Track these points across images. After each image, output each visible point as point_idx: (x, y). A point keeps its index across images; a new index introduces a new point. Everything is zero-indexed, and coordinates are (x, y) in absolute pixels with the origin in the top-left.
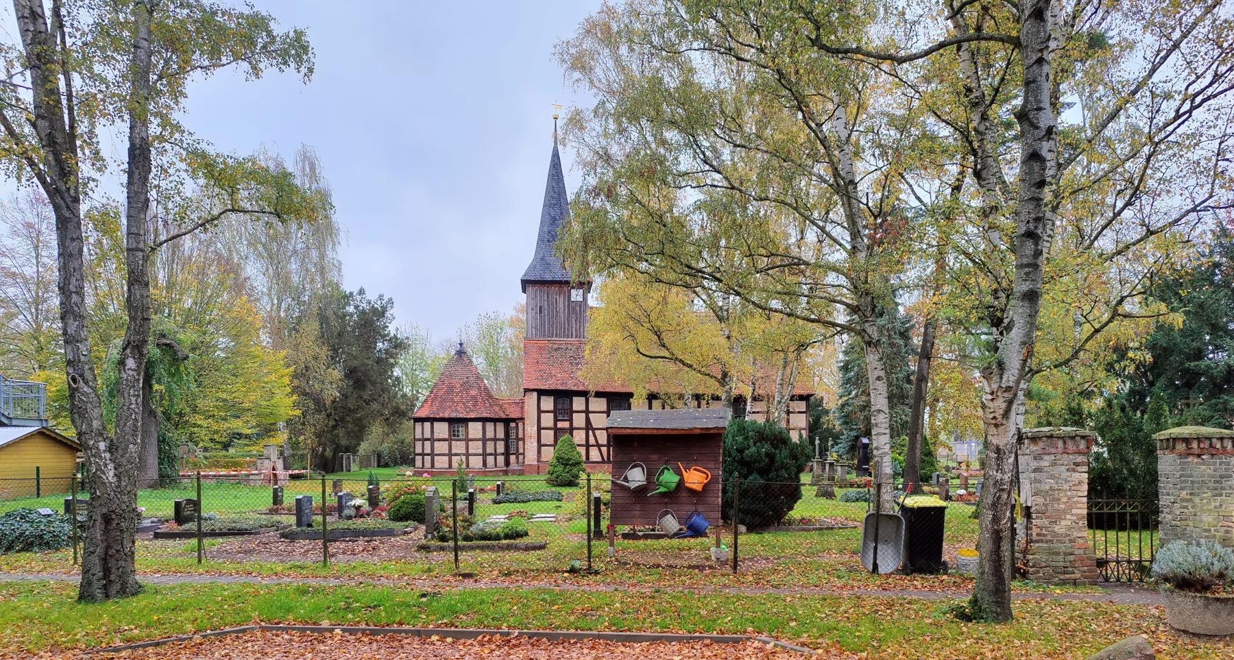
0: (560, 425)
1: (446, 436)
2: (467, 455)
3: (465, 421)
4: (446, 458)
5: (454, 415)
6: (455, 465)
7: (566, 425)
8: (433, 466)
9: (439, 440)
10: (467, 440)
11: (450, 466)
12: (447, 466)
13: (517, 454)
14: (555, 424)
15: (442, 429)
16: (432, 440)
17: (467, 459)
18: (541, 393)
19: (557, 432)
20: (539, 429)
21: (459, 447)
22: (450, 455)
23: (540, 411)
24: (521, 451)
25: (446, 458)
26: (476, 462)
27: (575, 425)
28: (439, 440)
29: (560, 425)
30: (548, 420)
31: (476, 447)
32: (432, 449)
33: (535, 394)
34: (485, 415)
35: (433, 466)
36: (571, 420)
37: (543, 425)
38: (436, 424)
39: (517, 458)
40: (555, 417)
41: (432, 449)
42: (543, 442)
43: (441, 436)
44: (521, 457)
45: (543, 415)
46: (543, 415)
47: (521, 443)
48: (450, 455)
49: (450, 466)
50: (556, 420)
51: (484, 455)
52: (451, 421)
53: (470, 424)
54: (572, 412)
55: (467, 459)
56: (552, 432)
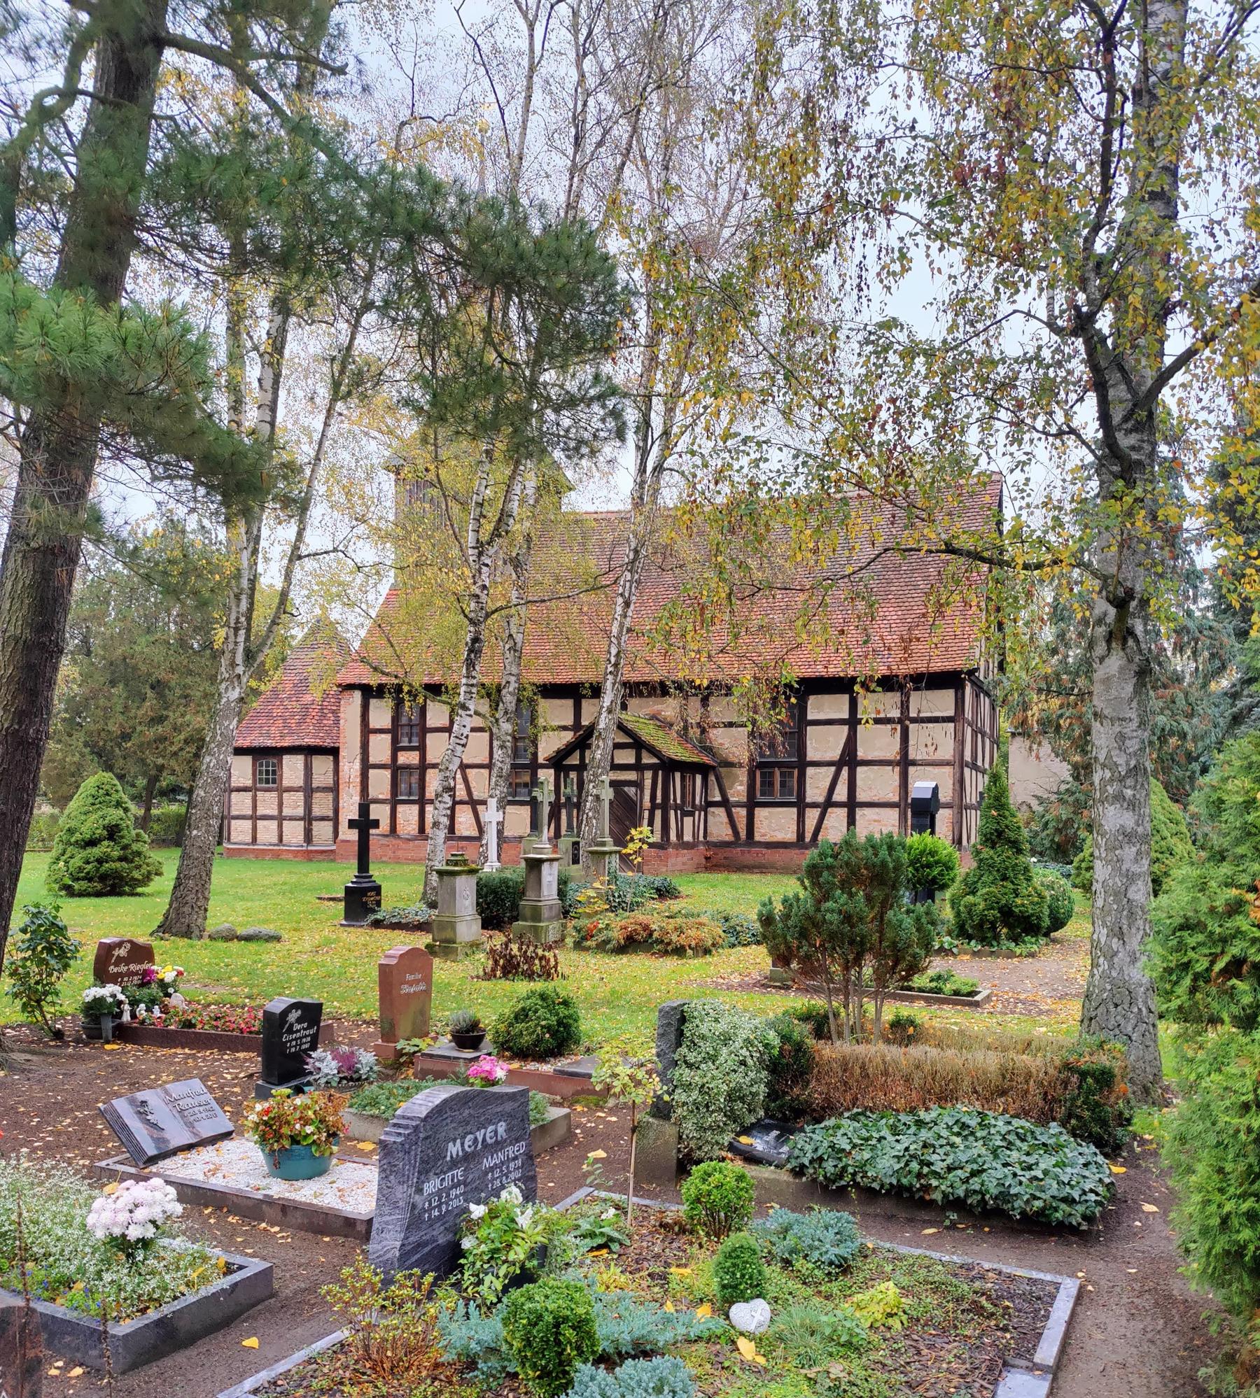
0: (403, 758)
1: (249, 783)
2: (280, 819)
4: (248, 824)
9: (239, 790)
10: (282, 790)
12: (249, 839)
14: (394, 757)
17: (280, 827)
18: (369, 692)
19: (396, 769)
20: (366, 766)
21: (268, 802)
22: (254, 818)
23: (366, 731)
25: (248, 824)
27: (431, 758)
28: (239, 790)
29: (403, 758)
30: (381, 748)
33: (357, 695)
34: (309, 741)
36: (422, 749)
37: (372, 760)
40: (395, 741)
42: (373, 793)
45: (372, 737)
46: (372, 737)
51: (308, 819)
52: (258, 753)
53: (286, 759)
54: (424, 730)
55: (280, 827)
56: (387, 774)
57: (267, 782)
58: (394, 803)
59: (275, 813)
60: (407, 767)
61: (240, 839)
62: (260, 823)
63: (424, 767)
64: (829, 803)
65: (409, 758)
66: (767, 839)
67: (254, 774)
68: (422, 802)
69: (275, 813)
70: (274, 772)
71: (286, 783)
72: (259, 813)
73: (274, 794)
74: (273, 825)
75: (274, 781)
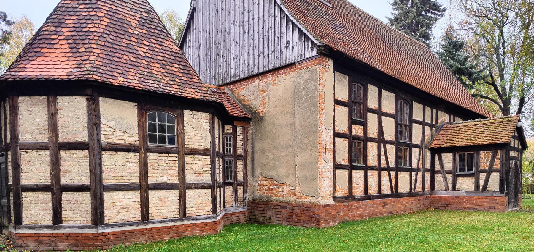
2: (182, 187)
3: (180, 104)
5: (153, 86)
6: (155, 212)
7: (358, 131)
8: (98, 216)
11: (145, 216)
12: (136, 216)
13: (234, 184)
15: (121, 120)
16: (94, 147)
17: (182, 198)
21: (163, 168)
22: (144, 187)
24: (240, 178)
25: (134, 197)
26: (199, 203)
28: (116, 148)
31: (199, 169)
32: (96, 170)
35: (98, 216)
36: (364, 124)
38: (108, 107)
39: (235, 191)
41: (96, 170)
43: (121, 138)
44: (240, 189)
47: (240, 164)
48: (144, 187)
49: (145, 216)
50: (352, 122)
52: (146, 100)
53: (188, 114)
55: (182, 198)
57: (162, 140)
58: (351, 168)
59: (175, 180)
60: (357, 138)
61: (123, 217)
62: (153, 196)
63: (366, 139)
64: (489, 172)
65: (358, 131)
66: (171, 191)
67: (141, 126)
68: (366, 169)
69: (175, 180)
70: (171, 129)
71: (189, 144)
72: (153, 179)
73: (174, 157)
74: (173, 196)
75: (172, 141)
